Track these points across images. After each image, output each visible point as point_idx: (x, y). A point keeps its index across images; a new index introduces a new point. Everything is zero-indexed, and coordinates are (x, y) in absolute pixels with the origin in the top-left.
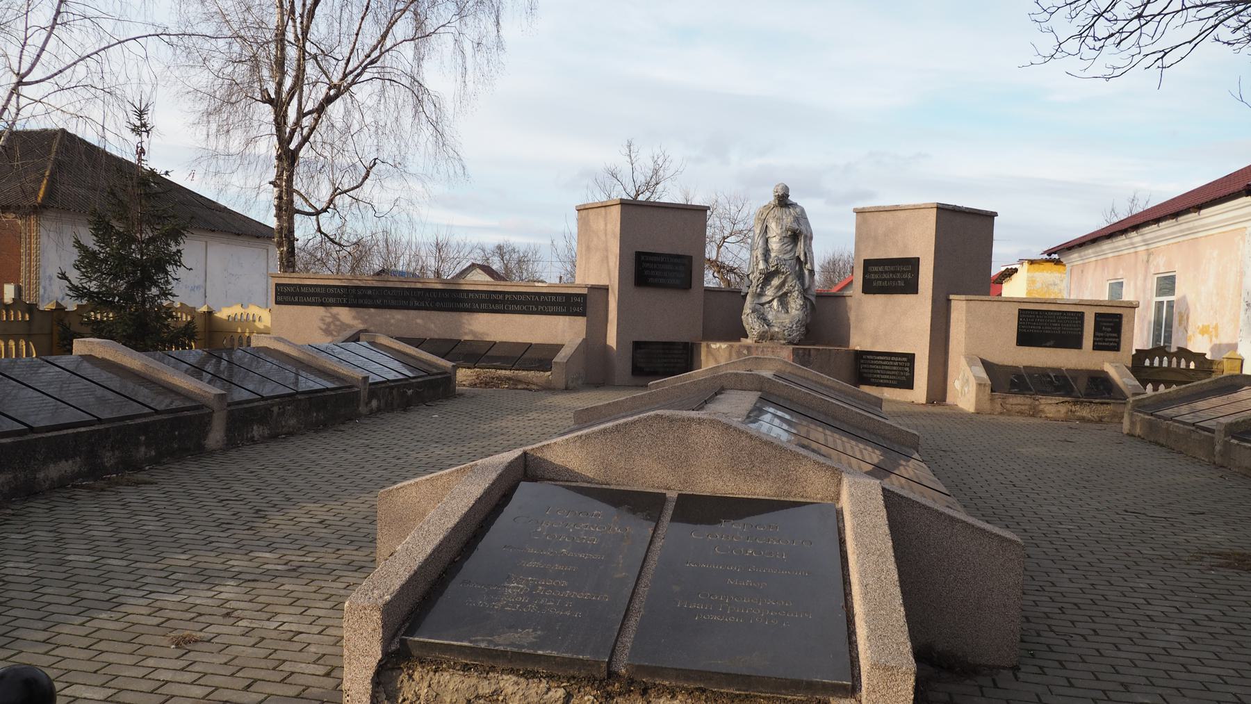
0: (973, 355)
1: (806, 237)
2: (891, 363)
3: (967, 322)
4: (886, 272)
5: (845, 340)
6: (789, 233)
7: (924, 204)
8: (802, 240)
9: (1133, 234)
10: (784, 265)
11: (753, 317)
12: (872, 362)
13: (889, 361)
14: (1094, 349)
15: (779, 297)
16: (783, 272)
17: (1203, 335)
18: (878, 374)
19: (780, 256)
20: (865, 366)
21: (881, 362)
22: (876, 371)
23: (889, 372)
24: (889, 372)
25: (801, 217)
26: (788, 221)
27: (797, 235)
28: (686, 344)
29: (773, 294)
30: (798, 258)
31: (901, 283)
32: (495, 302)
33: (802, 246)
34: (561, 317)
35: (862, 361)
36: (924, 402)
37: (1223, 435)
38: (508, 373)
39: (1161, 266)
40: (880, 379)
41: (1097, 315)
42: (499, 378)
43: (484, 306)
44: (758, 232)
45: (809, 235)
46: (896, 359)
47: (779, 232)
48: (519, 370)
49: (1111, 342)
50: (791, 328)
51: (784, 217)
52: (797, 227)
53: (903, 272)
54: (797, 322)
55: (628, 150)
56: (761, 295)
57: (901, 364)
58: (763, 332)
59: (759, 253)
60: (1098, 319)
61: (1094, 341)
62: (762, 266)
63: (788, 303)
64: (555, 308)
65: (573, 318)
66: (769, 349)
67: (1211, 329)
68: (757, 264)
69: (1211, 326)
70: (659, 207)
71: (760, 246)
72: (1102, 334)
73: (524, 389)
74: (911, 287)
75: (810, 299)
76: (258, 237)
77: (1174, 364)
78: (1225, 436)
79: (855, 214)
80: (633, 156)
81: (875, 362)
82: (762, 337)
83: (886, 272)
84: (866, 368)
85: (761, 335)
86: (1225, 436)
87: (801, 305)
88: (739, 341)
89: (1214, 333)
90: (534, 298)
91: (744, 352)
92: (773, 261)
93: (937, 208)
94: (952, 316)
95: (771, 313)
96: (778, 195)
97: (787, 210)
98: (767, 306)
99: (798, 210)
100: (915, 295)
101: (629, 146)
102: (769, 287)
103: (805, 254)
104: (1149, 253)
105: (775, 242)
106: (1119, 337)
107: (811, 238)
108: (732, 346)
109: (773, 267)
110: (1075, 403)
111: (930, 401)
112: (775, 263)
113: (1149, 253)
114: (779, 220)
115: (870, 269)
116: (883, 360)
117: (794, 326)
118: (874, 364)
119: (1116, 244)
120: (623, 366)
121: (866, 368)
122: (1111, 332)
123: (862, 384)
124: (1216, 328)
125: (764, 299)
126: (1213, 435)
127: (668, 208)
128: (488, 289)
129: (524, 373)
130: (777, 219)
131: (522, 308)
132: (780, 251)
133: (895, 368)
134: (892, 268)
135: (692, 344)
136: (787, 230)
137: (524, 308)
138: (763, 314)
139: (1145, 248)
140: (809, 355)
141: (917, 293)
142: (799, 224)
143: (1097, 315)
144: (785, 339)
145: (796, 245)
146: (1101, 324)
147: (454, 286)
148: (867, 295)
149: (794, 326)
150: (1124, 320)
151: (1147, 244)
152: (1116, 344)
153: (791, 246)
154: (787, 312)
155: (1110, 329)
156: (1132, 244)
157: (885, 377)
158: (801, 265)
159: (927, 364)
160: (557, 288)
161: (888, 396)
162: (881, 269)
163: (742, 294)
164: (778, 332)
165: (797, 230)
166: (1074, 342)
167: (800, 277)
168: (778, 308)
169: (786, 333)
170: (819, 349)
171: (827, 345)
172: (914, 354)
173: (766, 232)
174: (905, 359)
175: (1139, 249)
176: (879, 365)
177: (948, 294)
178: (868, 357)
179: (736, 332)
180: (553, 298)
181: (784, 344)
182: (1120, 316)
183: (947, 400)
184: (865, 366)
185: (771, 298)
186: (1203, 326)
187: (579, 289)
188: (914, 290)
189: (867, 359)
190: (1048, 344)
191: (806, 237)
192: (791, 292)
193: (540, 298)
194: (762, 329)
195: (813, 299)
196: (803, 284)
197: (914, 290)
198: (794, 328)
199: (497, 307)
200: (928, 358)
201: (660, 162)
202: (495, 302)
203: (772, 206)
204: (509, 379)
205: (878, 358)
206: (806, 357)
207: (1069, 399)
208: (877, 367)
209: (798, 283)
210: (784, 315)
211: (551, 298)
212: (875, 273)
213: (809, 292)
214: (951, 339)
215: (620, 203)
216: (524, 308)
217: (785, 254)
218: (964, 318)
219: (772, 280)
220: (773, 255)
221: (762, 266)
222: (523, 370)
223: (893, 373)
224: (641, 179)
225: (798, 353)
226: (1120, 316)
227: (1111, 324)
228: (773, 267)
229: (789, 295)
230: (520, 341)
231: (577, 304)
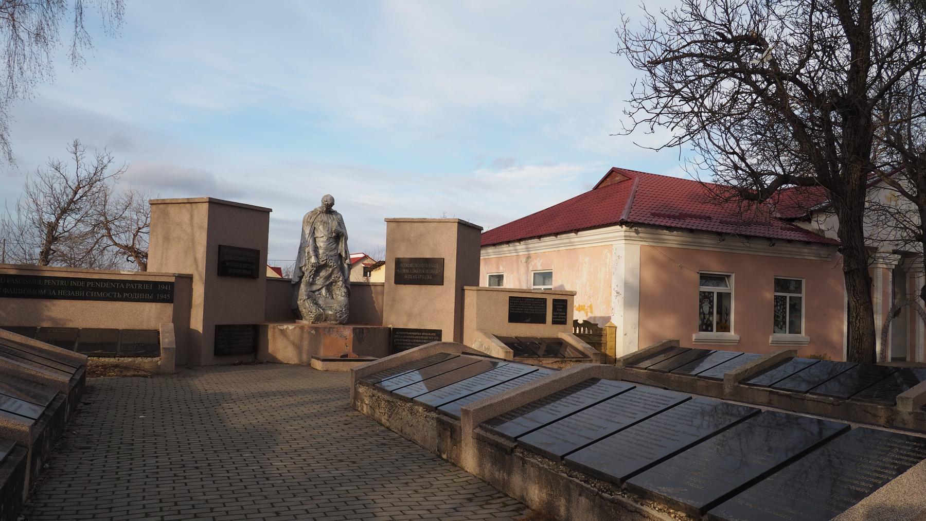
2: (422, 337)
6: (334, 234)
9: (518, 244)
12: (405, 337)
13: (420, 336)
14: (553, 324)
15: (328, 285)
16: (331, 266)
17: (580, 311)
22: (408, 344)
25: (341, 223)
26: (334, 225)
27: (339, 236)
28: (255, 325)
29: (322, 284)
30: (340, 255)
32: (75, 289)
33: (343, 246)
34: (148, 304)
35: (396, 336)
37: (732, 383)
38: (112, 360)
39: (539, 265)
41: (554, 301)
42: (105, 367)
43: (63, 293)
44: (308, 232)
46: (427, 334)
48: (124, 357)
49: (562, 318)
50: (341, 311)
51: (330, 222)
55: (74, 148)
56: (312, 284)
60: (554, 303)
61: (553, 318)
64: (141, 295)
65: (159, 305)
67: (586, 308)
69: (586, 306)
70: (247, 208)
72: (557, 313)
73: (134, 376)
74: (438, 280)
77: (586, 332)
78: (735, 382)
79: (386, 223)
80: (78, 154)
81: (408, 337)
82: (318, 319)
86: (735, 382)
87: (345, 292)
89: (589, 310)
91: (312, 332)
93: (458, 223)
94: (466, 301)
96: (328, 204)
98: (317, 293)
101: (76, 146)
102: (318, 278)
104: (529, 257)
105: (322, 242)
106: (566, 315)
110: (562, 362)
112: (325, 258)
113: (529, 257)
114: (324, 223)
116: (415, 336)
117: (344, 309)
118: (405, 339)
119: (501, 250)
120: (208, 348)
122: (561, 312)
124: (591, 307)
125: (315, 288)
126: (722, 382)
127: (256, 210)
128: (68, 276)
129: (130, 359)
131: (105, 294)
132: (326, 249)
135: (259, 325)
138: (315, 300)
139: (515, 254)
141: (443, 285)
143: (554, 301)
144: (337, 320)
145: (338, 244)
146: (557, 306)
147: (53, 272)
148: (398, 285)
150: (569, 303)
151: (528, 249)
152: (564, 320)
154: (333, 298)
155: (561, 310)
156: (516, 250)
158: (342, 263)
163: (292, 282)
166: (541, 320)
168: (326, 295)
170: (368, 328)
171: (367, 324)
173: (314, 232)
174: (434, 334)
175: (521, 253)
176: (411, 339)
179: (294, 315)
180: (140, 286)
182: (566, 301)
185: (320, 287)
186: (579, 305)
187: (166, 277)
190: (527, 321)
192: (336, 282)
193: (125, 286)
195: (349, 287)
199: (78, 293)
200: (453, 333)
201: (105, 161)
202: (75, 289)
203: (319, 212)
204: (116, 366)
207: (558, 359)
210: (331, 300)
211: (137, 286)
215: (209, 202)
216: (108, 295)
217: (330, 251)
220: (321, 251)
221: (313, 260)
222: (129, 357)
224: (83, 174)
225: (356, 332)
226: (566, 301)
227: (562, 307)
229: (334, 284)
230: (102, 327)
231: (165, 292)
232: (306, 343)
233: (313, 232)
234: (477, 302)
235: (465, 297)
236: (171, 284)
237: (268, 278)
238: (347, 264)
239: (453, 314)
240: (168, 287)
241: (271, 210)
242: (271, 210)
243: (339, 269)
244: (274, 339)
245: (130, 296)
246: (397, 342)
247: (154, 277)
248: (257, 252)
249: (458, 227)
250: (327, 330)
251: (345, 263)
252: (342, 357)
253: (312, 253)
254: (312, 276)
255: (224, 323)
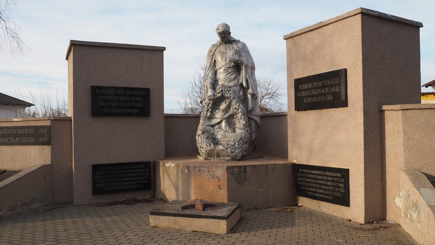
0: (415, 170)
1: (247, 66)
2: (326, 178)
3: (405, 134)
4: (314, 88)
5: (284, 155)
7: (346, 13)
8: (244, 69)
10: (229, 91)
11: (202, 137)
16: (228, 97)
18: (313, 187)
19: (226, 84)
20: (302, 179)
21: (316, 177)
22: (311, 185)
23: (323, 187)
24: (323, 187)
26: (230, 54)
30: (241, 85)
31: (330, 98)
34: (33, 147)
35: (299, 174)
36: (363, 223)
40: (316, 192)
45: (250, 65)
46: (330, 174)
47: (224, 63)
50: (233, 145)
52: (237, 58)
53: (331, 86)
54: (239, 140)
56: (211, 118)
57: (335, 179)
58: (210, 150)
59: (208, 83)
62: (210, 93)
63: (234, 124)
65: (41, 147)
66: (205, 169)
68: (207, 92)
71: (209, 77)
75: (254, 120)
76: (7, 104)
79: (286, 40)
81: (311, 176)
82: (209, 155)
83: (314, 88)
84: (303, 181)
85: (208, 153)
88: (197, 158)
90: (13, 131)
91: (185, 171)
92: (219, 88)
95: (220, 133)
97: (230, 45)
98: (217, 127)
99: (240, 45)
100: (344, 108)
102: (217, 111)
103: (247, 81)
107: (253, 68)
108: (178, 166)
109: (219, 93)
111: (369, 220)
112: (220, 90)
114: (223, 54)
115: (300, 87)
116: (318, 175)
117: (237, 144)
118: (308, 178)
121: (303, 181)
123: (301, 196)
125: (214, 121)
130: (222, 53)
131: (5, 140)
133: (329, 183)
134: (320, 84)
136: (230, 61)
137: (7, 140)
138: (213, 134)
140: (245, 172)
142: (240, 56)
144: (228, 156)
148: (300, 112)
149: (237, 144)
153: (235, 75)
157: (321, 191)
159: (363, 181)
160: (28, 122)
161: (324, 210)
162: (310, 86)
164: (222, 150)
165: (238, 60)
167: (244, 101)
168: (226, 128)
169: (229, 150)
170: (254, 166)
172: (348, 170)
173: (215, 65)
174: (339, 175)
177: (380, 105)
178: (304, 170)
181: (228, 161)
183: (388, 218)
184: (302, 179)
185: (219, 120)
187: (44, 122)
188: (344, 104)
189: (304, 173)
191: (247, 66)
193: (16, 132)
194: (209, 148)
195: (257, 119)
196: (246, 107)
197: (344, 104)
198: (236, 146)
200: (363, 174)
203: (219, 44)
205: (313, 172)
206: (242, 174)
208: (313, 181)
209: (241, 105)
210: (230, 134)
211: (24, 131)
212: (305, 90)
213: (253, 113)
214: (387, 151)
217: (229, 82)
218: (401, 130)
219: (220, 105)
221: (210, 93)
223: (329, 188)
228: (219, 93)
229: (235, 116)
232: (180, 184)
233: (214, 64)
234: (404, 128)
235: (386, 122)
236: (49, 128)
237: (166, 115)
238: (250, 94)
239: (363, 147)
240: (45, 131)
241: (164, 49)
242: (164, 49)
243: (237, 99)
244: (164, 177)
245: (20, 140)
246: (300, 181)
247: (36, 122)
248: (147, 91)
249: (362, 19)
250: (197, 169)
251: (248, 92)
252: (184, 208)
253: (209, 85)
254: (210, 110)
255: (104, 162)
